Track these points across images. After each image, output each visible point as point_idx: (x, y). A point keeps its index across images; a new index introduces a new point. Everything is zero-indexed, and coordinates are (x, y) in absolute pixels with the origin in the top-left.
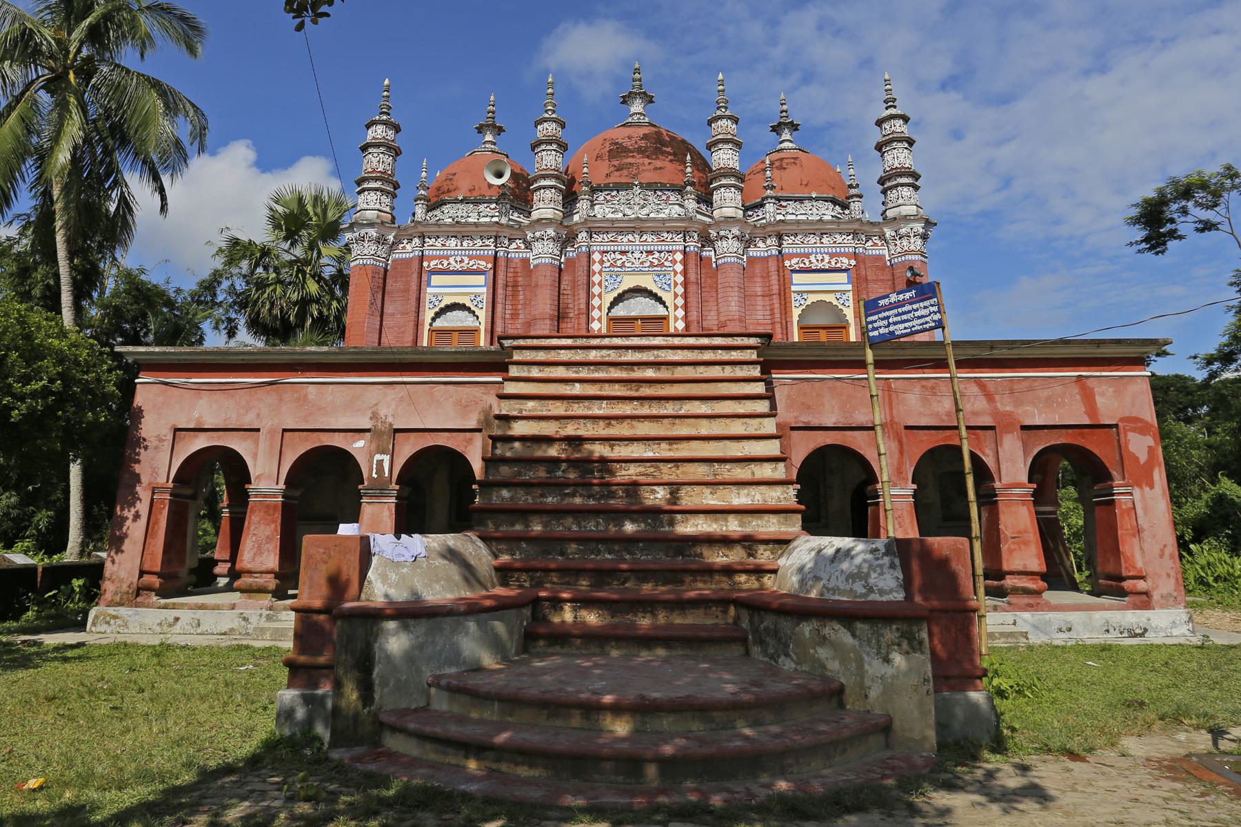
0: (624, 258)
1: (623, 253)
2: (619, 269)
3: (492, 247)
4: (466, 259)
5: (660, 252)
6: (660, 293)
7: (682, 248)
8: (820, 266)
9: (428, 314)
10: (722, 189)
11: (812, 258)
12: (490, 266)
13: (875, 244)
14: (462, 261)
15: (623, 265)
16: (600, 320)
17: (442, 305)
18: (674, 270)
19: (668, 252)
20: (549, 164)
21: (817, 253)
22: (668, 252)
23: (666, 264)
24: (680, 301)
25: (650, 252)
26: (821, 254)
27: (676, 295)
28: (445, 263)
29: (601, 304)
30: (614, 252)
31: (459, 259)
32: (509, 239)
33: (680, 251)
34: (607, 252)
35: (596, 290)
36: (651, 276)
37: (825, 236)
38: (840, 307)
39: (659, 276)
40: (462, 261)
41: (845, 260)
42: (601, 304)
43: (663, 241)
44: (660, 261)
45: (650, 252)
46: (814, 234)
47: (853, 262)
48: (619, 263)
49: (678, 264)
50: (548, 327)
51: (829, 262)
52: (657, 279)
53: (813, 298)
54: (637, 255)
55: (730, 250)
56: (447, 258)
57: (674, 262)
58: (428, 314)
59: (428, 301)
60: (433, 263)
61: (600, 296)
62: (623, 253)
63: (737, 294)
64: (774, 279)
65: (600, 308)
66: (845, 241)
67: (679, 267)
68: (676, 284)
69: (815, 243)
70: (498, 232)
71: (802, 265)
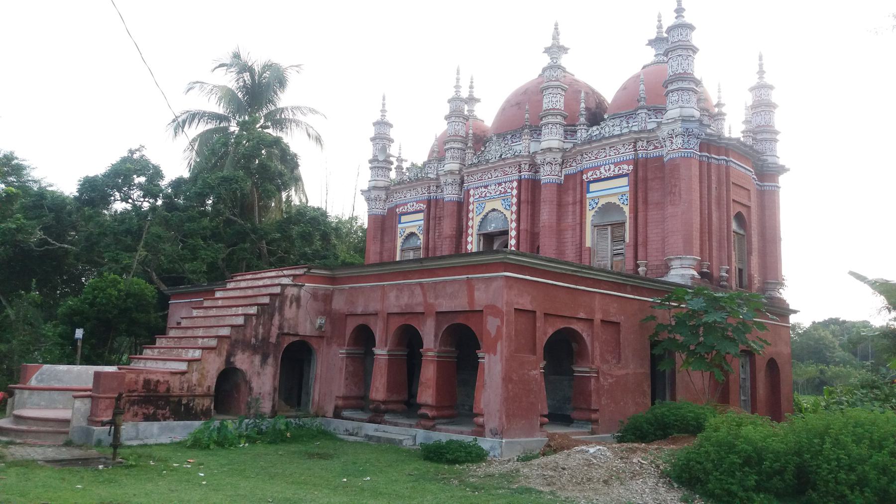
0: (486, 190)
1: (486, 187)
2: (483, 199)
3: (426, 194)
4: (415, 203)
5: (505, 183)
6: (505, 212)
7: (517, 177)
8: (607, 175)
9: (399, 241)
10: (550, 125)
11: (602, 170)
12: (425, 206)
13: (656, 148)
14: (413, 206)
15: (486, 196)
16: (472, 235)
17: (405, 234)
18: (512, 194)
19: (510, 182)
20: (450, 132)
21: (605, 165)
22: (510, 182)
23: (509, 191)
24: (514, 217)
25: (500, 184)
26: (608, 164)
27: (512, 213)
28: (406, 207)
29: (472, 225)
30: (481, 187)
31: (412, 204)
32: (436, 186)
33: (516, 180)
34: (477, 188)
35: (470, 215)
36: (500, 201)
37: (612, 149)
38: (622, 206)
39: (504, 200)
40: (413, 206)
41: (625, 167)
42: (472, 225)
43: (507, 174)
44: (505, 189)
45: (500, 184)
46: (605, 149)
47: (631, 167)
48: (484, 194)
49: (515, 190)
50: (448, 243)
51: (614, 171)
52: (503, 203)
53: (603, 202)
54: (493, 187)
55: (545, 174)
56: (406, 204)
57: (512, 189)
58: (399, 241)
59: (399, 232)
60: (401, 209)
61: (472, 219)
62: (486, 187)
63: (548, 206)
64: (578, 192)
65: (472, 227)
66: (627, 151)
67: (515, 192)
68: (512, 204)
69: (605, 156)
70: (429, 183)
71: (595, 176)
